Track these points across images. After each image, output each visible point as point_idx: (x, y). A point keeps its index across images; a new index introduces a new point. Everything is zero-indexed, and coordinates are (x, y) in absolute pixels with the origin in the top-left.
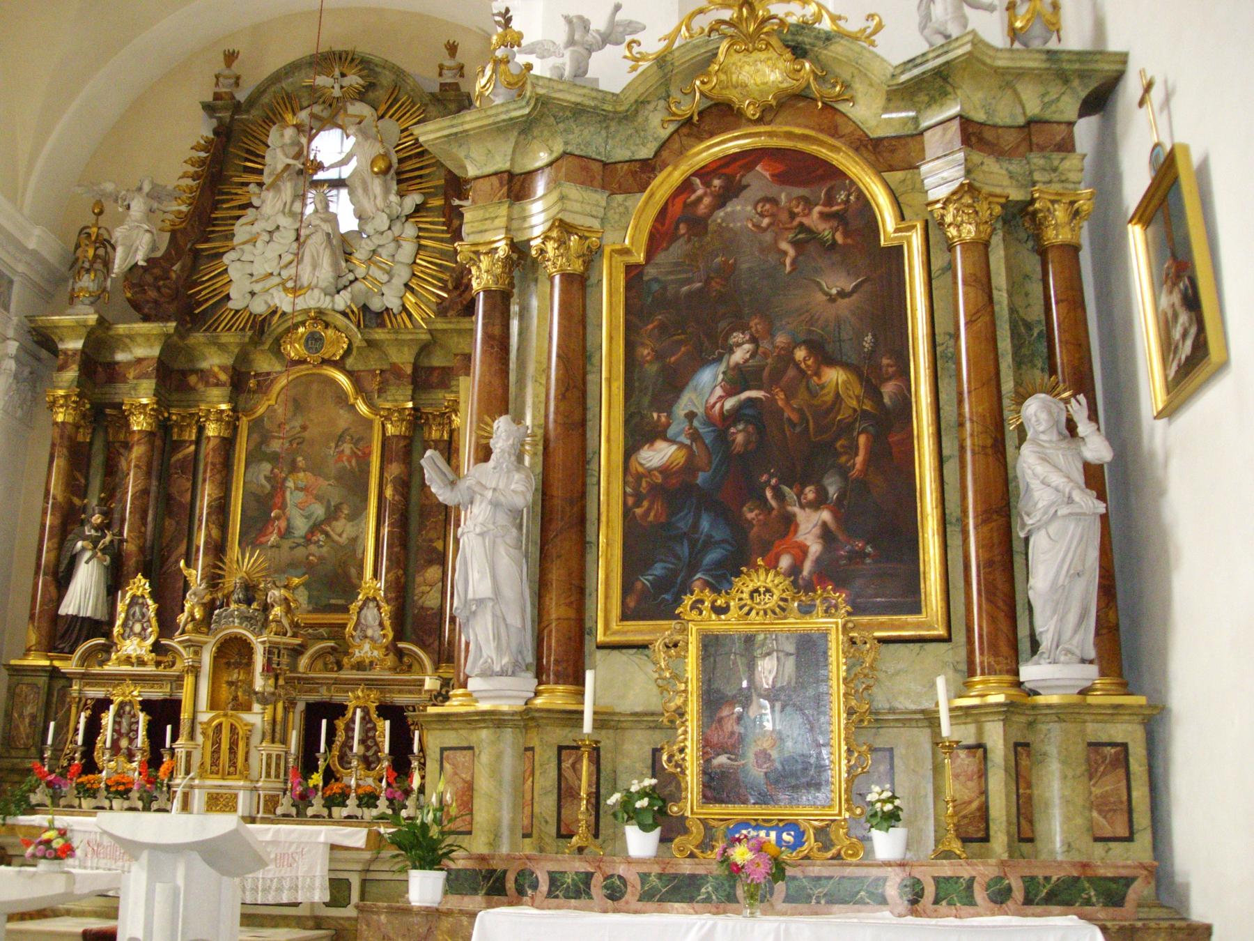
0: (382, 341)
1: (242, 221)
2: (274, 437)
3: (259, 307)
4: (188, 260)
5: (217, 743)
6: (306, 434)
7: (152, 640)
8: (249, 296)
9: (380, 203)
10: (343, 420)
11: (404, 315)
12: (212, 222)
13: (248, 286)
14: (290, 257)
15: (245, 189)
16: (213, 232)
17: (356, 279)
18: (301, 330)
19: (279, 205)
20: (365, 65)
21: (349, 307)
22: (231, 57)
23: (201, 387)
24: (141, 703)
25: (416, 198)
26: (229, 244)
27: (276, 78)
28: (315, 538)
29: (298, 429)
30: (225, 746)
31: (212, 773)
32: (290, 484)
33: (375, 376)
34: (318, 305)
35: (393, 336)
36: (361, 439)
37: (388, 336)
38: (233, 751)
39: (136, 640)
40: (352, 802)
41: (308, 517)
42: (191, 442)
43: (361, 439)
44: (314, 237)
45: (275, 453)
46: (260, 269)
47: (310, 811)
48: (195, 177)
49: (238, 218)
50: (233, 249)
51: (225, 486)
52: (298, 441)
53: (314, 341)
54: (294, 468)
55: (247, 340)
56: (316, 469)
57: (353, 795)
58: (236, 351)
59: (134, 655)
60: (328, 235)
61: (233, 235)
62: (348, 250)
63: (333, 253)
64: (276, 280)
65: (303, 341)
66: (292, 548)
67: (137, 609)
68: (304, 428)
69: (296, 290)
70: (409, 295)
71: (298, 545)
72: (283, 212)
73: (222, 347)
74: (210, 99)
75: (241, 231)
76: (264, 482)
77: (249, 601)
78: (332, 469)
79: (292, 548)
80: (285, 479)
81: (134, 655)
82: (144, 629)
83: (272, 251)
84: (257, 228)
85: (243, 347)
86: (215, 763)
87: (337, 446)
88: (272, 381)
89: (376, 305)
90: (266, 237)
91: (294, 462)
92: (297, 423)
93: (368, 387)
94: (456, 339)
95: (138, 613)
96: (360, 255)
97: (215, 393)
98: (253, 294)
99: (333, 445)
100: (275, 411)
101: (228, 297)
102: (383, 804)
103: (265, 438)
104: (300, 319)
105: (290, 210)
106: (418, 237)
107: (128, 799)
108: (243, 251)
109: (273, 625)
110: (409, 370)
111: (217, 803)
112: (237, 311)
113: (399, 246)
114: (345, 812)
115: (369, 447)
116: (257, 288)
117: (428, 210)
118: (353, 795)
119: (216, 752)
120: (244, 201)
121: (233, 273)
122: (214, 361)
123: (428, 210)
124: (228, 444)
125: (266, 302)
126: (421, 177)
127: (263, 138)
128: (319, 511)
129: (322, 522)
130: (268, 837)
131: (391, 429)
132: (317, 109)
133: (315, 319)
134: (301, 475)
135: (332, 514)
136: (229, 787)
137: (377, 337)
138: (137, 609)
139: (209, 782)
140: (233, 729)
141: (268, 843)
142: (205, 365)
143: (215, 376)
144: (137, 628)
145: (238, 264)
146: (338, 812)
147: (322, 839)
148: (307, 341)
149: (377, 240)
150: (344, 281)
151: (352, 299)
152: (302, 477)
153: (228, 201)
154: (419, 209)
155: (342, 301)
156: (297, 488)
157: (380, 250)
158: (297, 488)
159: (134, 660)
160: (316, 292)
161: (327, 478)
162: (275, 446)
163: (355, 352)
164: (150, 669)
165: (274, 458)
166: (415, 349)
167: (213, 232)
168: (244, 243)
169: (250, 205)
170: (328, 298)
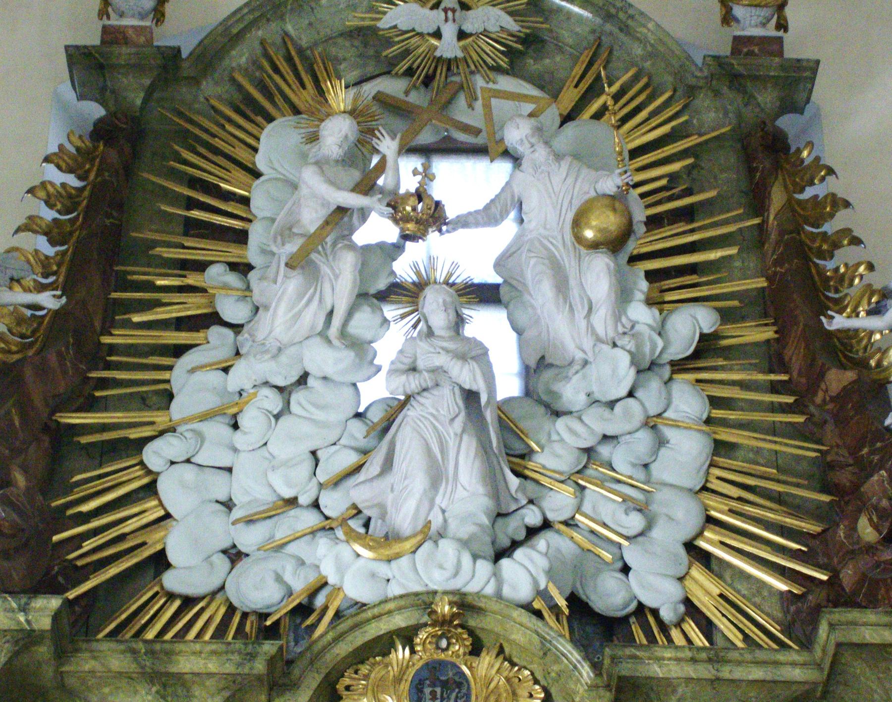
0: (668, 684)
3: (259, 589)
4: (36, 454)
8: (222, 563)
9: (602, 320)
11: (691, 627)
12: (101, 356)
13: (221, 531)
15: (192, 279)
16: (104, 383)
17: (547, 524)
18: (401, 653)
19: (313, 316)
21: (543, 594)
25: (704, 319)
26: (160, 419)
34: (457, 584)
35: (704, 671)
37: (690, 671)
44: (426, 400)
46: (251, 488)
48: (54, 233)
49: (179, 351)
50: (173, 430)
55: (260, 666)
60: (470, 397)
61: (170, 396)
62: (518, 448)
63: (484, 447)
64: (309, 519)
65: (405, 686)
70: (698, 573)
72: (323, 335)
74: (94, 39)
75: (193, 384)
83: (291, 440)
84: (242, 375)
89: (609, 595)
90: (273, 401)
96: (555, 453)
98: (234, 555)
101: (160, 562)
104: (400, 621)
105: (343, 334)
106: (709, 421)
108: (200, 437)
112: (188, 601)
113: (661, 442)
116: (248, 539)
117: (727, 352)
120: (193, 306)
121: (174, 491)
123: (727, 352)
125: (279, 579)
126: (692, 269)
127: (242, 154)
133: (444, 622)
137: (656, 670)
145: (188, 473)
149: (600, 422)
150: (513, 528)
151: (550, 573)
154: (707, 346)
155: (522, 574)
157: (605, 451)
160: (448, 548)
167: (104, 383)
168: (206, 417)
169: (214, 319)
170: (484, 567)
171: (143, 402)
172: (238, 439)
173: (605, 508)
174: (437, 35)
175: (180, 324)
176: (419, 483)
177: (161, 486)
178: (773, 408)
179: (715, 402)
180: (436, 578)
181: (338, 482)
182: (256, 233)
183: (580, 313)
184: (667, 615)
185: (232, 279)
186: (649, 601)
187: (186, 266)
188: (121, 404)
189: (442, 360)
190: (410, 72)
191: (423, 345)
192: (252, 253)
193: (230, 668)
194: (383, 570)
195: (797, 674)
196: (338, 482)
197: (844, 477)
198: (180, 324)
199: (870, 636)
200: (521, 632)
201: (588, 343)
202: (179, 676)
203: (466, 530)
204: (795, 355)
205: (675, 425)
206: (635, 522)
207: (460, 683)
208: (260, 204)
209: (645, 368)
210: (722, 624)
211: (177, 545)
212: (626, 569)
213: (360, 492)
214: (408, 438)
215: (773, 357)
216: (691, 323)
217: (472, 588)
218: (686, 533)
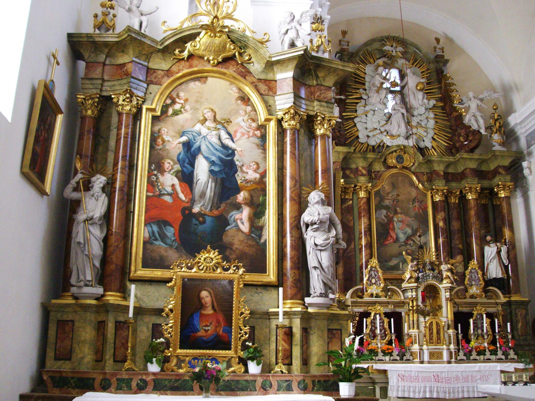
0: (434, 161)
1: (359, 105)
2: (386, 199)
3: (373, 142)
5: (431, 329)
6: (399, 198)
7: (382, 285)
8: (366, 138)
9: (420, 102)
10: (414, 193)
13: (366, 133)
14: (385, 122)
15: (358, 91)
18: (395, 153)
19: (378, 99)
20: (401, 42)
22: (344, 33)
23: (352, 176)
24: (384, 313)
27: (366, 44)
28: (409, 243)
29: (395, 196)
30: (435, 331)
31: (430, 343)
32: (395, 219)
33: (424, 175)
35: (440, 159)
36: (422, 201)
38: (438, 333)
39: (375, 286)
40: (488, 353)
41: (405, 234)
42: (350, 200)
43: (422, 201)
45: (387, 206)
46: (370, 126)
47: (472, 358)
49: (357, 103)
51: (370, 219)
52: (396, 201)
53: (400, 159)
54: (396, 213)
56: (406, 213)
57: (487, 350)
58: (371, 161)
59: (375, 293)
64: (379, 132)
66: (399, 247)
67: (373, 272)
68: (398, 195)
69: (392, 136)
70: (433, 142)
71: (402, 245)
73: (365, 158)
75: (360, 109)
76: (384, 218)
77: (433, 270)
78: (413, 213)
79: (399, 247)
80: (393, 217)
81: (375, 293)
82: (376, 281)
83: (375, 119)
84: (367, 108)
85: (375, 159)
86: (431, 339)
87: (413, 204)
88: (381, 175)
89: (422, 145)
91: (396, 210)
92: (395, 193)
93: (422, 180)
94: (468, 162)
95: (373, 275)
97: (362, 179)
98: (368, 136)
99: (411, 203)
100: (384, 188)
101: (358, 137)
102: (500, 353)
103: (382, 199)
104: (395, 149)
106: (435, 118)
107: (391, 355)
109: (448, 280)
110: (442, 174)
111: (435, 356)
112: (362, 144)
113: (428, 121)
114: (486, 357)
115: (426, 204)
116: (370, 134)
118: (487, 350)
119: (431, 334)
120: (358, 96)
122: (360, 164)
124: (368, 199)
126: (430, 93)
128: (409, 231)
129: (411, 236)
130: (477, 369)
131: (437, 198)
132: (385, 59)
134: (400, 215)
135: (414, 233)
136: (439, 349)
138: (373, 272)
139: (430, 347)
140: (437, 324)
141: (477, 371)
142: (353, 166)
143: (361, 171)
144: (373, 281)
145: (361, 123)
146: (482, 357)
147: (499, 368)
148: (397, 158)
150: (408, 134)
152: (400, 217)
153: (352, 95)
154: (434, 106)
156: (398, 221)
158: (398, 221)
159: (374, 295)
160: (401, 138)
161: (410, 217)
162: (387, 203)
163: (416, 164)
164: (383, 299)
165: (387, 208)
166: (445, 164)
169: (361, 98)
170: (406, 141)
171: (352, 111)
172: (367, 118)
173: (421, 131)
174: (392, 51)
175: (356, 99)
176: (397, 127)
177: (357, 125)
178: (443, 116)
179: (435, 115)
180: (400, 143)
181: (382, 126)
182: (367, 84)
183: (417, 101)
184: (430, 148)
185: (364, 92)
186: (427, 146)
187: (356, 88)
188: (349, 112)
189: (399, 108)
190: (388, 57)
191: (396, 106)
192: (367, 87)
193: (375, 157)
194: (392, 141)
195: (452, 160)
196: (382, 126)
197: (454, 128)
198: (356, 99)
199: (464, 156)
200: (411, 151)
201: (418, 105)
202: (368, 158)
203: (403, 135)
204: (447, 108)
205: (430, 118)
206: (425, 134)
207: (402, 158)
208: (367, 79)
209: (426, 109)
210: (437, 149)
211: (360, 136)
212: (424, 141)
213: (387, 127)
214: (393, 119)
215: (443, 108)
216: (433, 102)
217: (405, 144)
218: (432, 136)
